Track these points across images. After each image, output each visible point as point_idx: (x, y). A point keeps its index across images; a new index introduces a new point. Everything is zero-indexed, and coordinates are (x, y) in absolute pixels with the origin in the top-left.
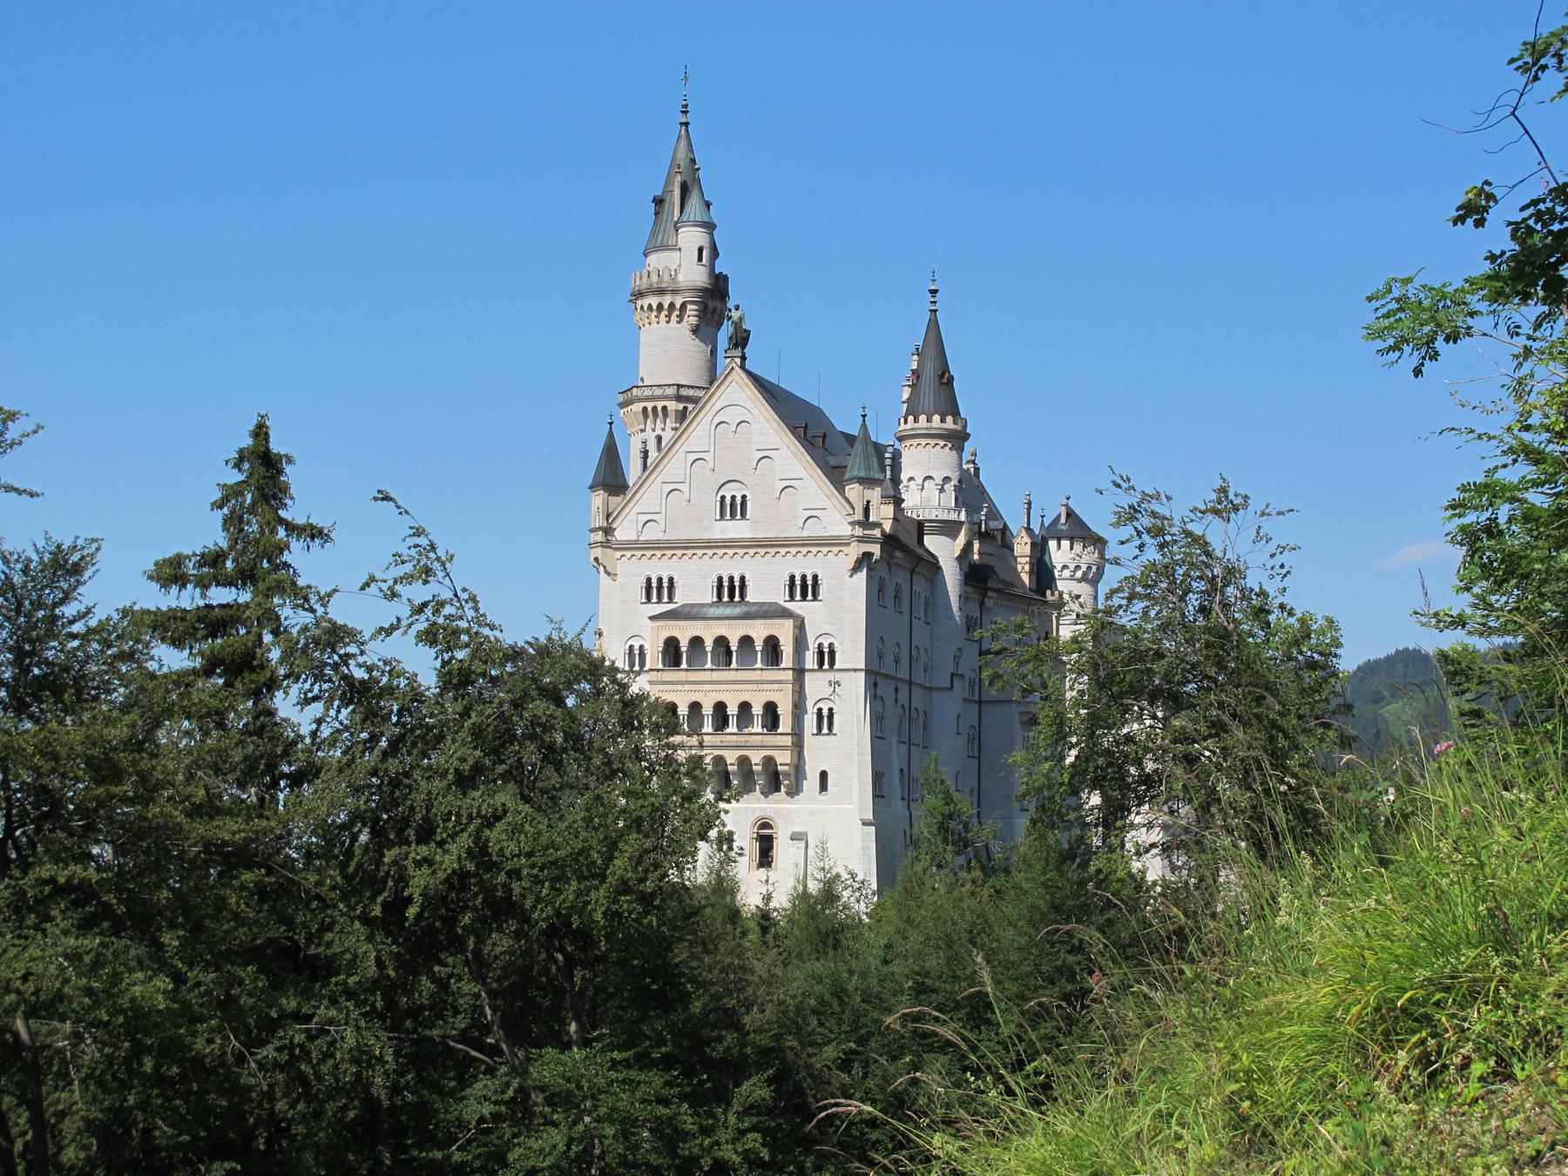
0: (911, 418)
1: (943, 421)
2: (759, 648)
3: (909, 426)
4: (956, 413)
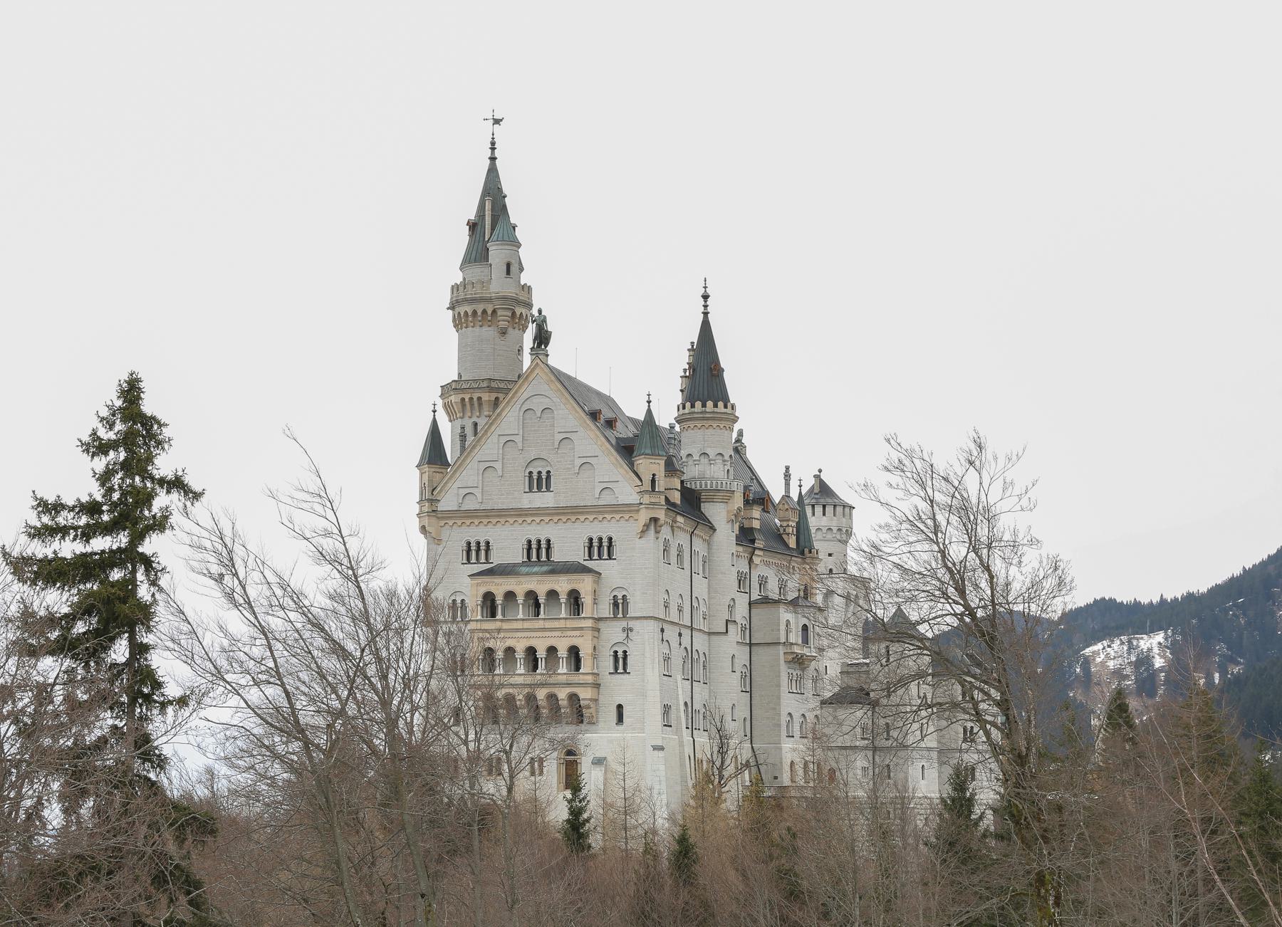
0: (688, 405)
1: (716, 406)
3: (687, 411)
4: (726, 400)
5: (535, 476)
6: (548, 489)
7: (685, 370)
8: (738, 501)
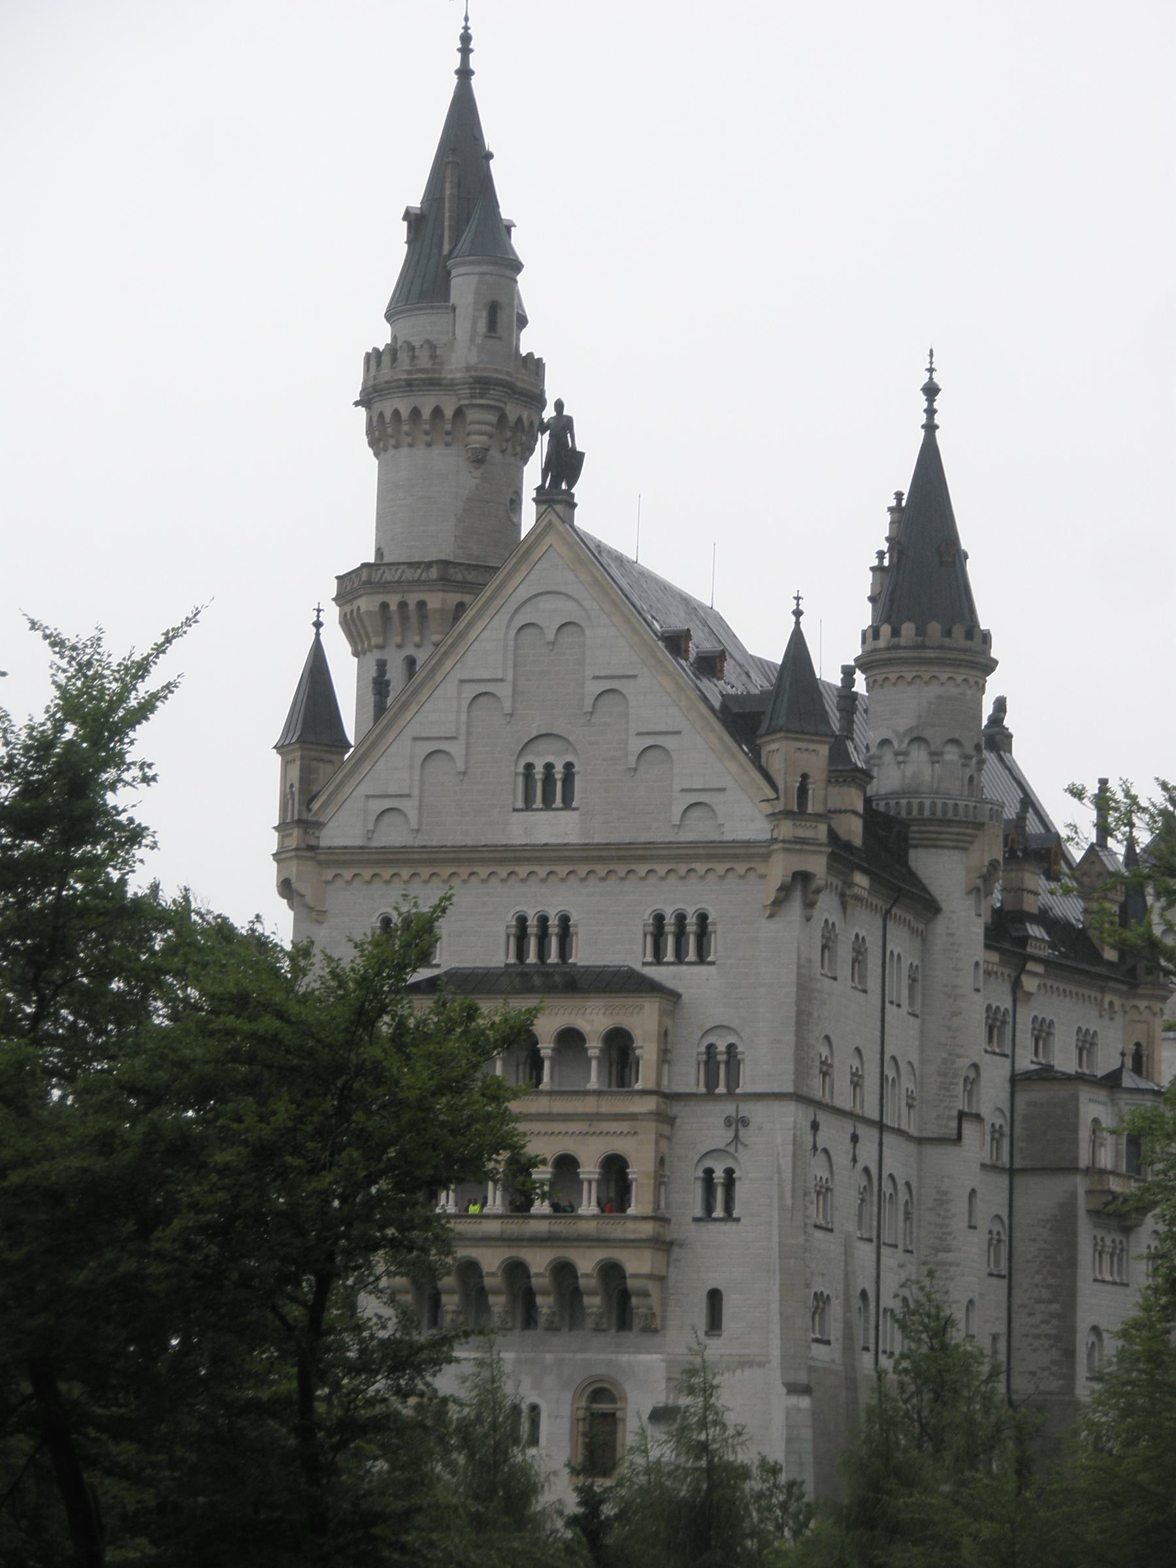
0: (886, 629)
2: (593, 1052)
5: (539, 771)
6: (567, 803)
7: (881, 555)
8: (991, 848)
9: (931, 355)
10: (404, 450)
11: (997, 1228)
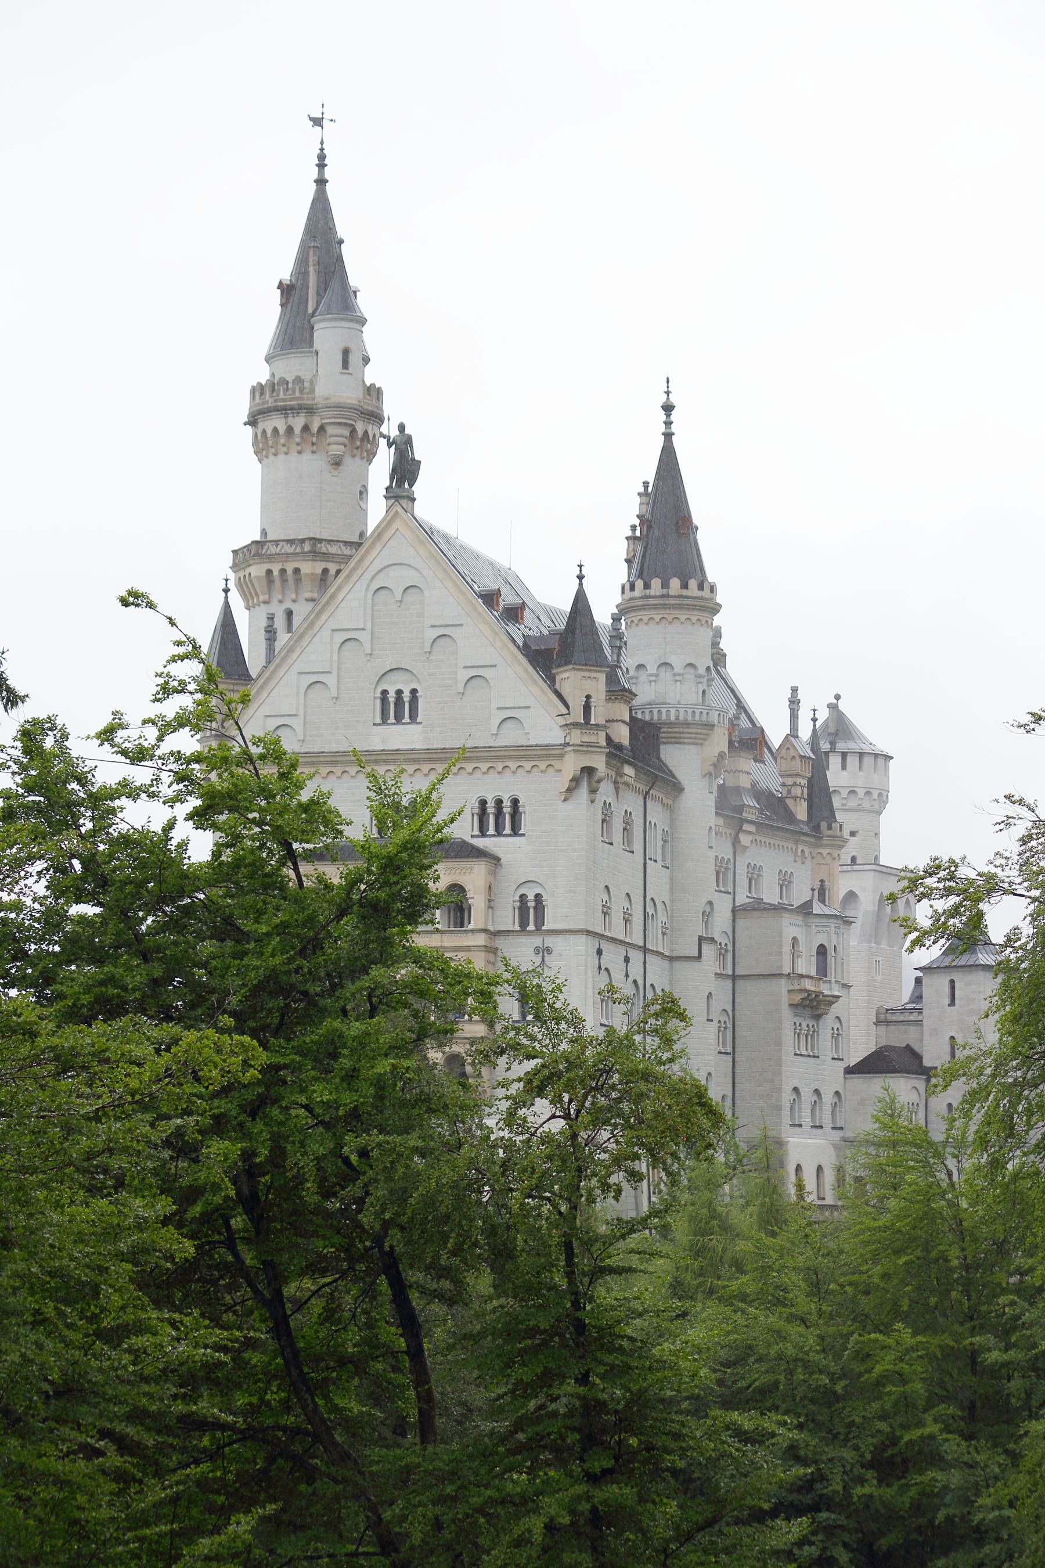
0: (639, 584)
1: (685, 586)
5: (392, 697)
7: (634, 528)
8: (719, 742)
9: (668, 382)
10: (281, 457)
11: (723, 1019)
